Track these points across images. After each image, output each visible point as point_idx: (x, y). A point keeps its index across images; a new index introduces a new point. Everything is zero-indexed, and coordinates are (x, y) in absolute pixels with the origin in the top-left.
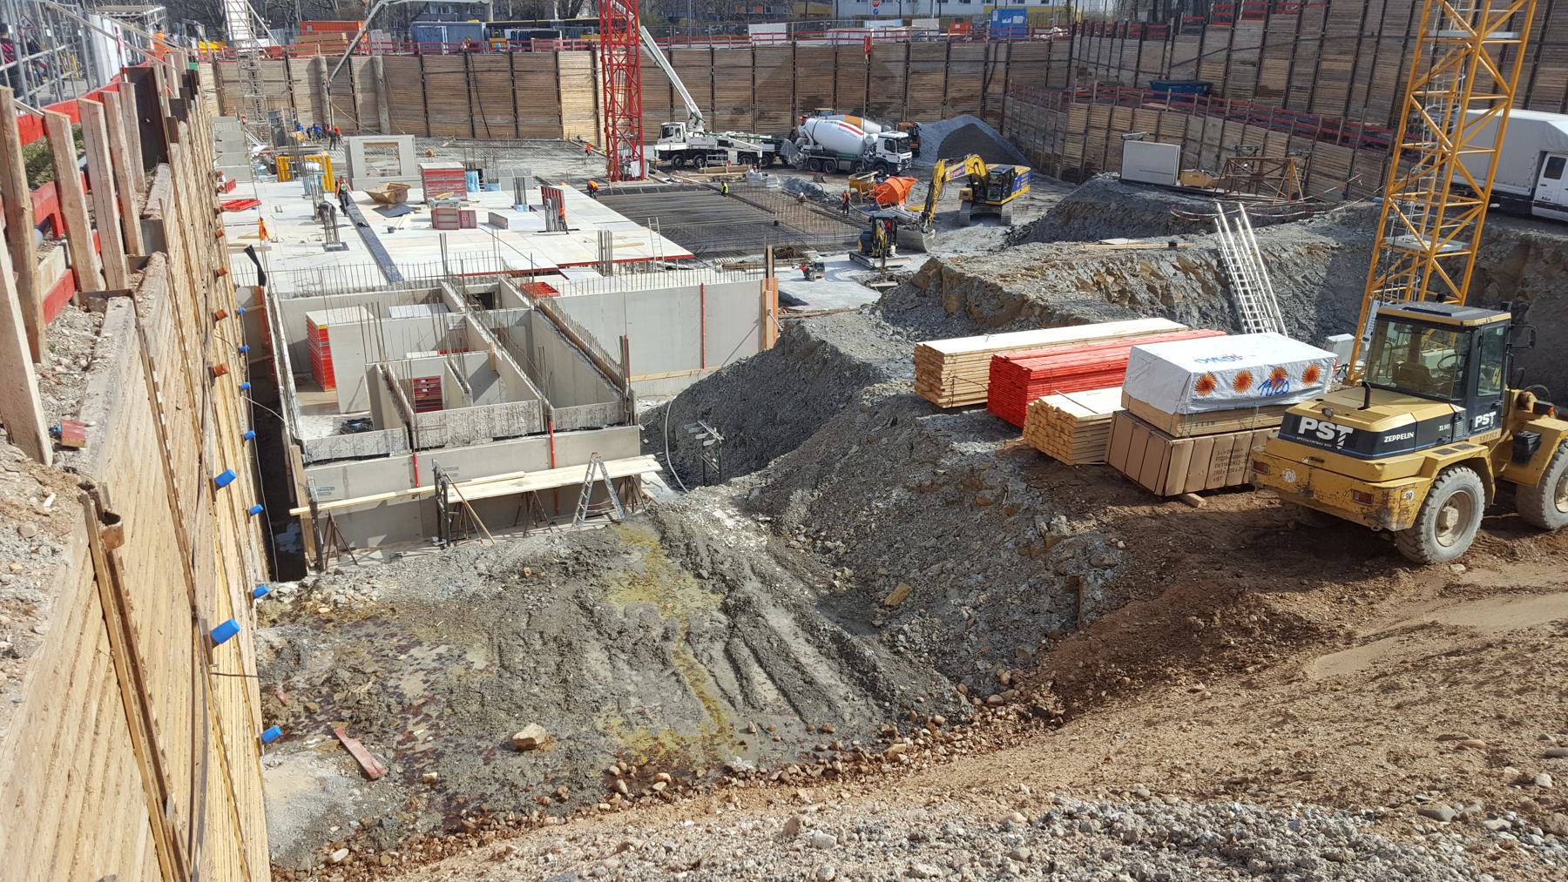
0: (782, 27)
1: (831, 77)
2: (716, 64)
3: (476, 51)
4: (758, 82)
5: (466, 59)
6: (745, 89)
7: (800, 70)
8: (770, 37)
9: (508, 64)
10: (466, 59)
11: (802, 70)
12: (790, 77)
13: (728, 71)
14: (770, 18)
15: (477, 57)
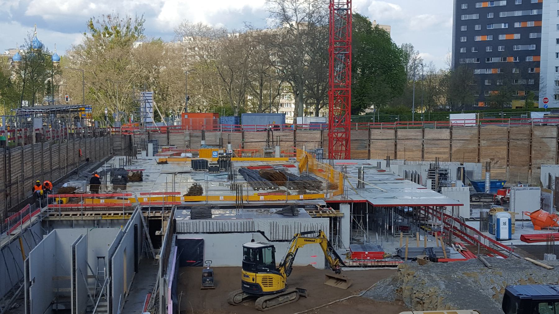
0: (473, 116)
1: (506, 147)
2: (425, 138)
3: (277, 130)
4: (454, 149)
5: (269, 134)
6: (444, 153)
7: (483, 143)
8: (463, 122)
9: (293, 137)
10: (269, 134)
11: (485, 142)
12: (475, 146)
13: (433, 142)
14: (468, 110)
15: (276, 133)
